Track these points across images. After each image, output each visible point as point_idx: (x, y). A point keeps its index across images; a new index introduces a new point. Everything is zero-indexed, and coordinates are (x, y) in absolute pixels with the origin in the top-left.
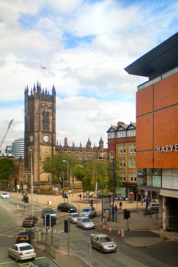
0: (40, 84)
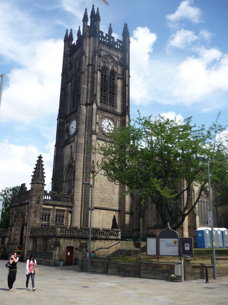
0: (98, 9)
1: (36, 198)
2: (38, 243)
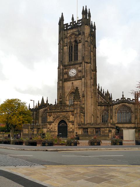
0: (89, 10)
2: (89, 130)
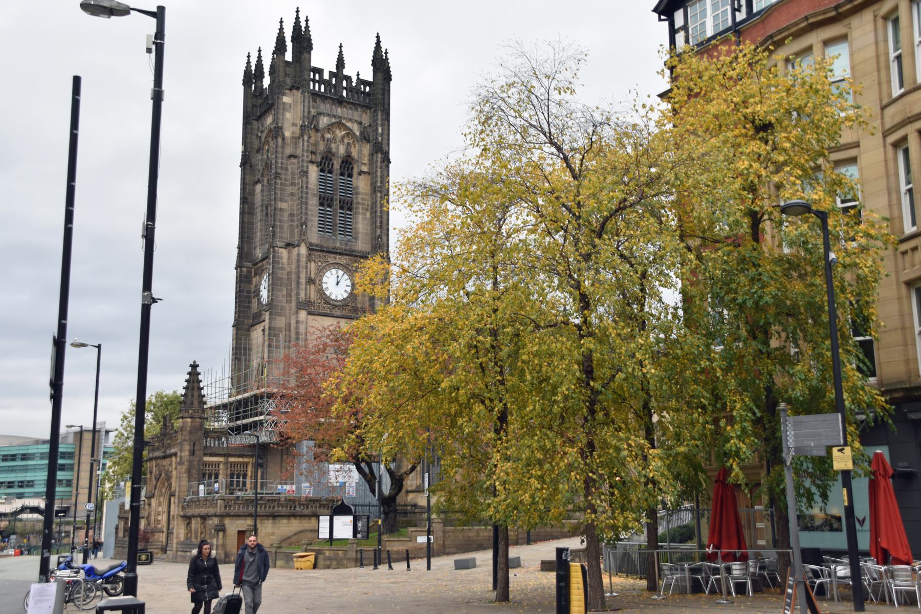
0: (307, 21)
1: (190, 445)
